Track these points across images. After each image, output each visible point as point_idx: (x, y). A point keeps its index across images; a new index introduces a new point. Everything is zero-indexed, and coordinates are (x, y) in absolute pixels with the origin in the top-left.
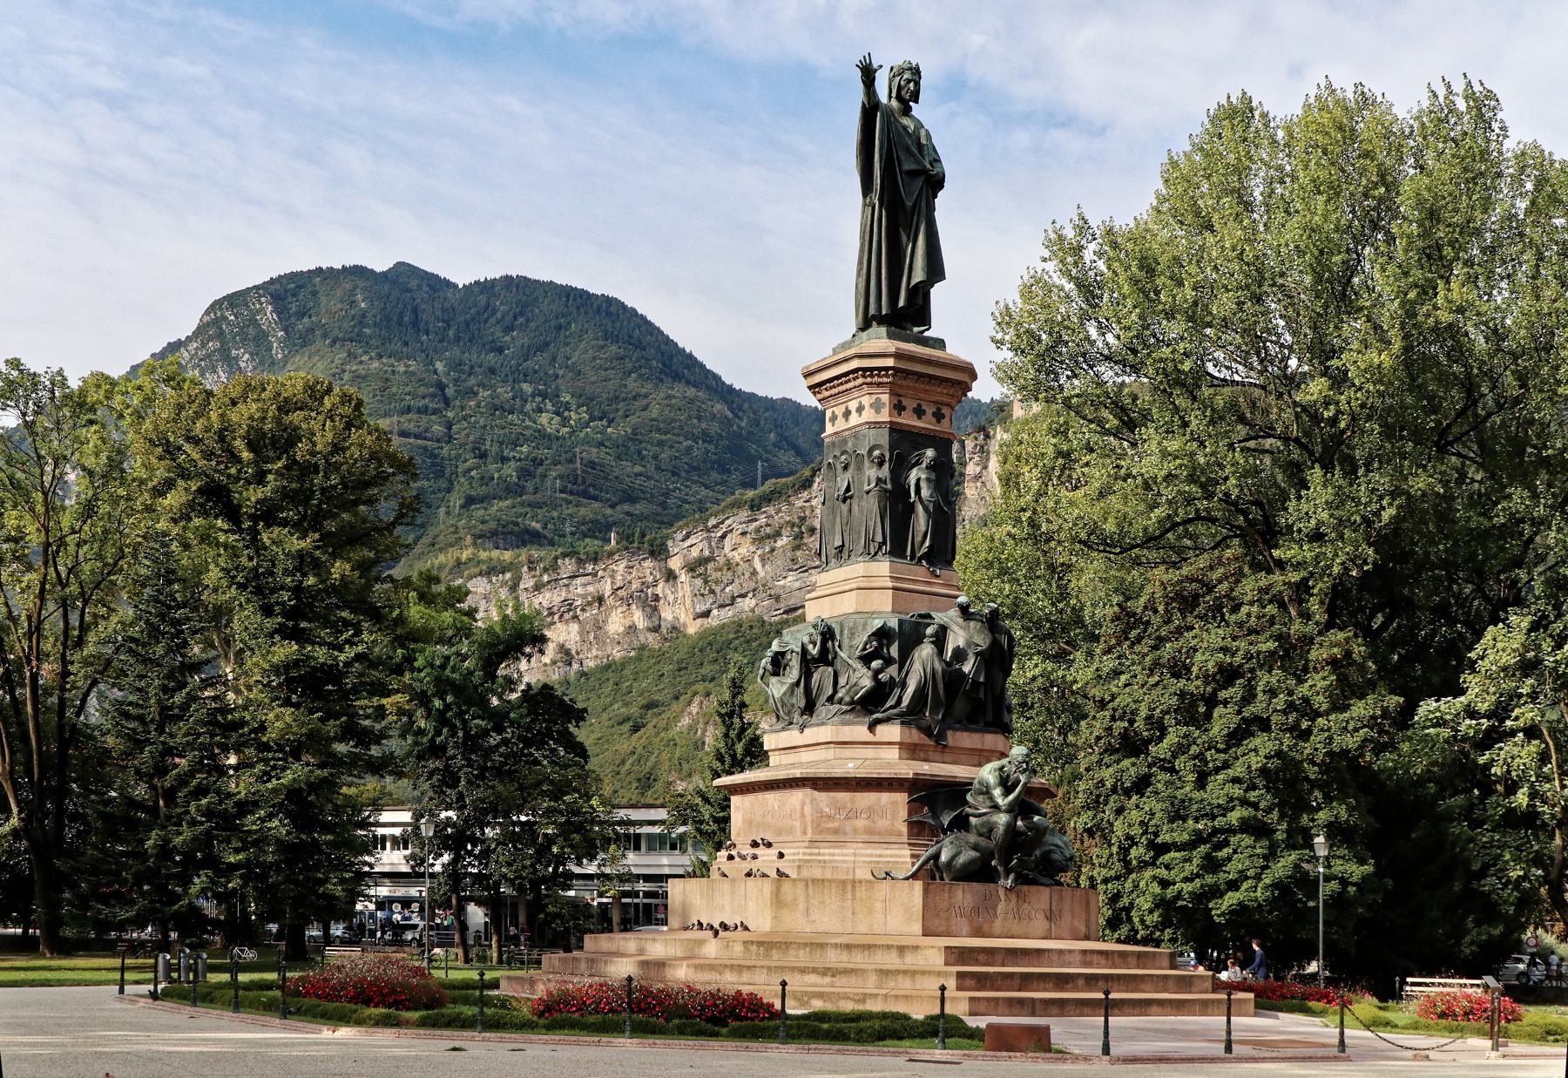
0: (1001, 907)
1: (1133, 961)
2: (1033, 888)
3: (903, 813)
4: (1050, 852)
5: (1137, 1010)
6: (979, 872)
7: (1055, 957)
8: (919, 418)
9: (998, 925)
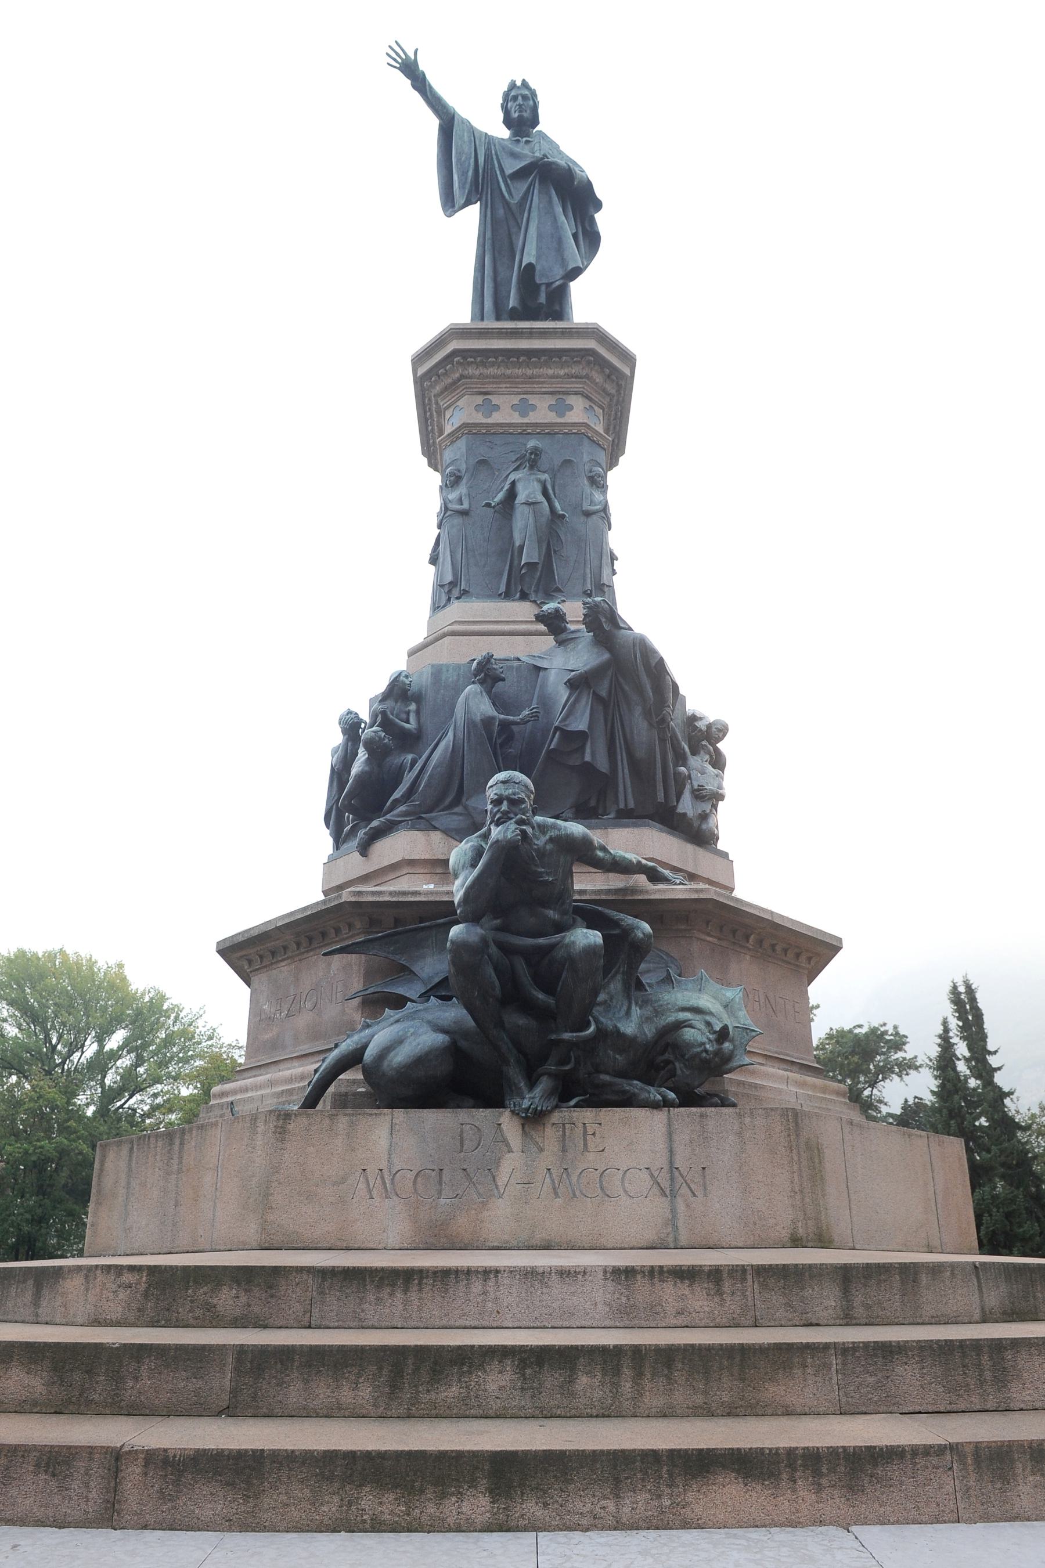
0: (511, 1166)
1: (827, 1299)
2: (619, 1112)
3: (357, 984)
4: (679, 1025)
5: (637, 1501)
6: (453, 1081)
7: (509, 1294)
8: (524, 414)
9: (499, 1216)
